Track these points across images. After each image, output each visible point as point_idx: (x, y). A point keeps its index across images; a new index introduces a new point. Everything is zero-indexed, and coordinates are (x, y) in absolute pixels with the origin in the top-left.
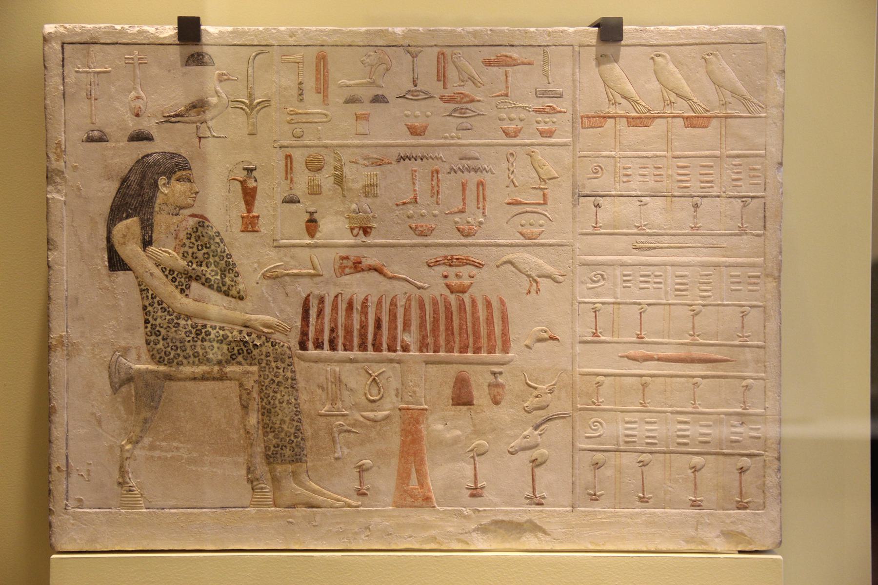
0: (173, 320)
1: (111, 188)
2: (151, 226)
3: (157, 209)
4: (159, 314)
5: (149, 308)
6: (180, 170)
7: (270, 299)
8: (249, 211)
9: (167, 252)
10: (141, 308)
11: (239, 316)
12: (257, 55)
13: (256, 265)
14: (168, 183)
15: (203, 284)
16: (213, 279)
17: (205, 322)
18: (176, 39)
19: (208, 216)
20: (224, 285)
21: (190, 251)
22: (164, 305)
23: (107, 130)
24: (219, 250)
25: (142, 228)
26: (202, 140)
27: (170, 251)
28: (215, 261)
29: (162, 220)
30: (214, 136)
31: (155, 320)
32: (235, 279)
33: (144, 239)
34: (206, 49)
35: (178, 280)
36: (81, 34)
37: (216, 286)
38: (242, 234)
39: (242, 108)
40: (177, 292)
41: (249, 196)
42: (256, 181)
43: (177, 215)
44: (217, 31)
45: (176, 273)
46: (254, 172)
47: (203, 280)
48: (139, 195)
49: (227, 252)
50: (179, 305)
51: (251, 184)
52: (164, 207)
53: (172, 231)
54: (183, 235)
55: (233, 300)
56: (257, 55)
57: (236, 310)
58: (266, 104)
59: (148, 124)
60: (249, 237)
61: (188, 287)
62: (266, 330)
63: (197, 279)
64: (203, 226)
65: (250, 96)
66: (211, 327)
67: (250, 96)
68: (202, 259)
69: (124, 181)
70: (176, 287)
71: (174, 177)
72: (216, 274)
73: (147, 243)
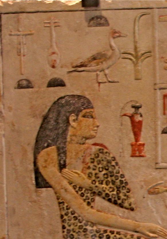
0: (82, 226)
1: (34, 125)
2: (65, 153)
3: (68, 139)
4: (73, 221)
5: (65, 217)
6: (85, 109)
7: (154, 210)
8: (137, 140)
9: (77, 172)
10: (59, 215)
11: (130, 223)
13: (143, 183)
14: (77, 119)
15: (104, 198)
16: (111, 194)
17: (106, 228)
18: (81, 6)
19: (106, 144)
20: (119, 199)
21: (94, 172)
22: (76, 215)
23: (31, 79)
24: (115, 171)
25: (59, 155)
26: (102, 85)
27: (79, 172)
28: (112, 181)
29: (72, 148)
30: (110, 82)
31: (70, 226)
32: (127, 194)
33: (60, 163)
34: (104, 13)
35: (86, 195)
36: (13, 5)
37: (113, 199)
38: (133, 159)
39: (130, 59)
40: (85, 204)
41: (137, 128)
42: (141, 116)
43: (83, 144)
45: (84, 189)
46: (140, 110)
47: (104, 195)
48: (56, 129)
49: (121, 173)
50: (86, 214)
51: (138, 118)
52: (74, 138)
53: (80, 157)
54: (88, 160)
55: (126, 211)
57: (128, 218)
58: (149, 53)
59: (60, 73)
60: (136, 161)
61: (93, 200)
62: (151, 235)
63: (100, 194)
64: (102, 153)
65: (136, 48)
66: (111, 232)
67: (136, 48)
68: (102, 179)
69: (45, 118)
70: (84, 200)
71: (81, 114)
72: (113, 191)
73: (62, 166)
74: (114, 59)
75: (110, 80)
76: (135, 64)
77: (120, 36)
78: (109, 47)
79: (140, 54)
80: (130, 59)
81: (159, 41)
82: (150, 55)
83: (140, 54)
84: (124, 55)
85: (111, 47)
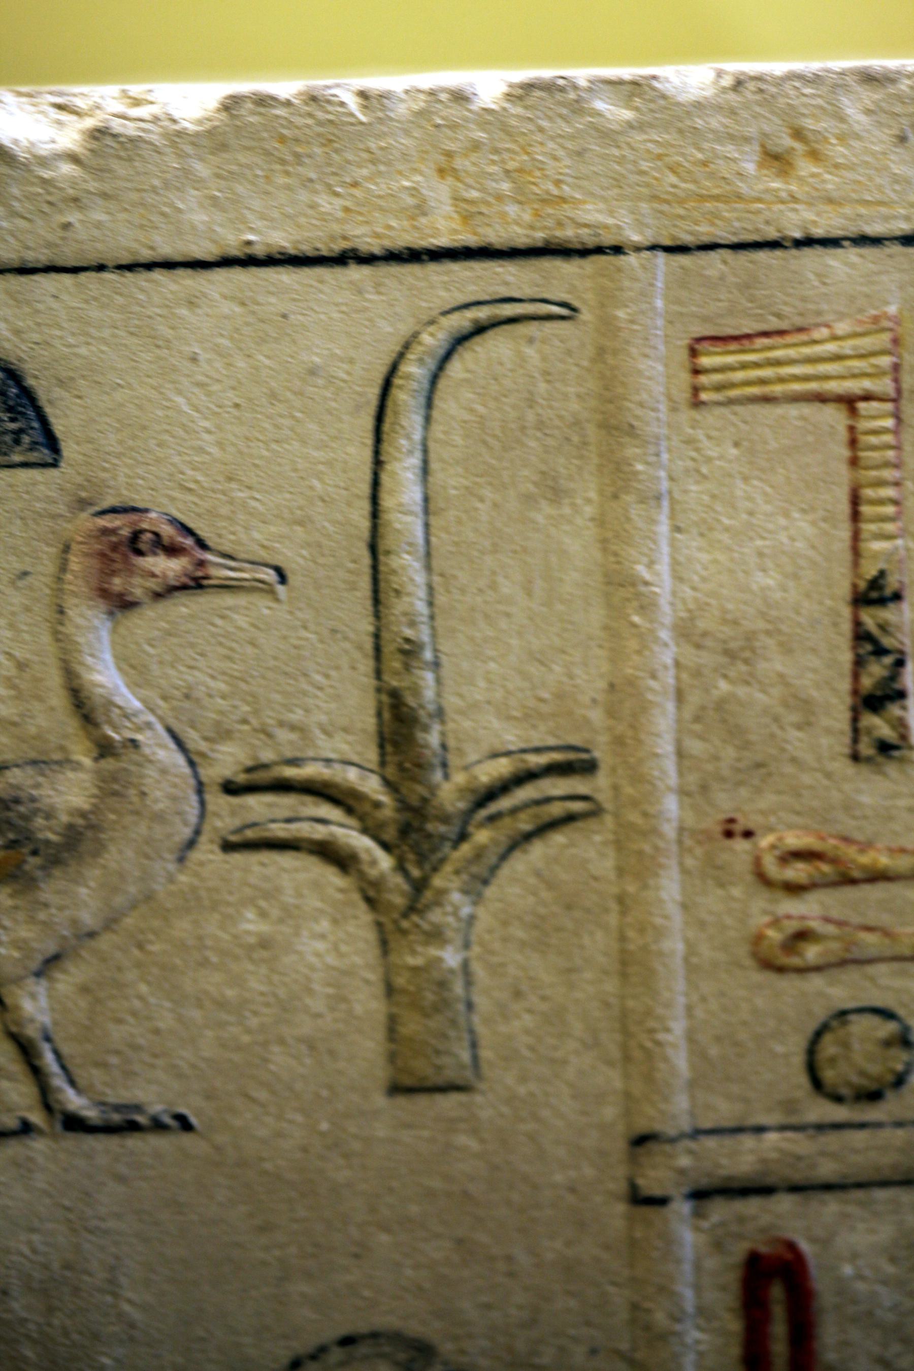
12: (461, 340)
30: (74, 1123)
39: (330, 854)
44: (69, 136)
56: (461, 340)
58: (555, 787)
65: (399, 727)
67: (399, 727)
74: (119, 856)
75: (74, 1101)
76: (398, 917)
77: (196, 584)
78: (52, 717)
79: (449, 792)
80: (330, 854)
81: (684, 631)
82: (577, 806)
83: (449, 792)
84: (257, 805)
85: (84, 707)
